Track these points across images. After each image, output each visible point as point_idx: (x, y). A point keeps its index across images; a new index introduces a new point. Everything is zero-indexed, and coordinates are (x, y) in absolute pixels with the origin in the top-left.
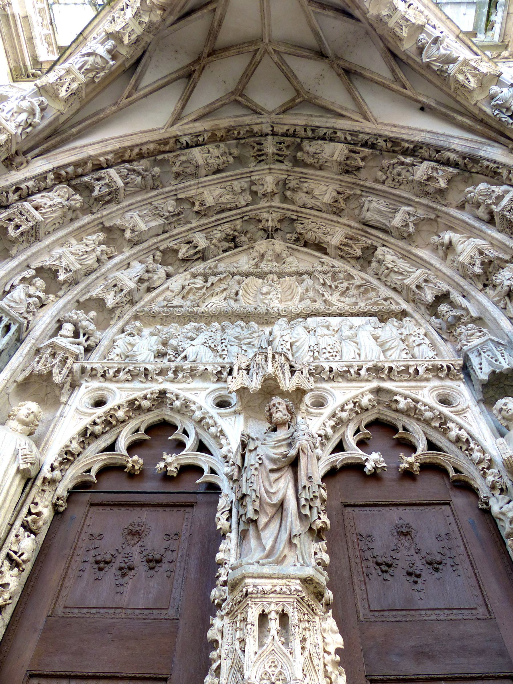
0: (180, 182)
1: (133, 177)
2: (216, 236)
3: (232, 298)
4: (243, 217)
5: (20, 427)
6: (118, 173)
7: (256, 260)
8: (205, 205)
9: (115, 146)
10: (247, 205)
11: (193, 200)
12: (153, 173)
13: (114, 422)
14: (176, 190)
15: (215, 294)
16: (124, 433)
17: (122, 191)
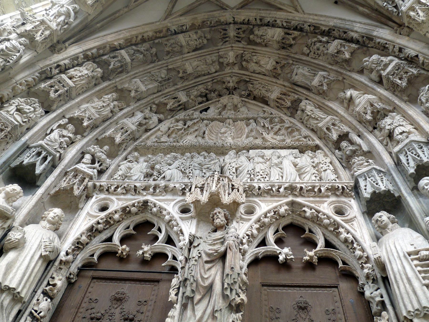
0: (170, 58)
1: (137, 55)
2: (193, 93)
3: (201, 136)
4: (213, 80)
5: (48, 226)
7: (219, 110)
8: (187, 73)
10: (216, 72)
11: (179, 69)
12: (151, 52)
13: (112, 222)
14: (167, 63)
15: (189, 133)
16: (118, 230)
17: (129, 65)
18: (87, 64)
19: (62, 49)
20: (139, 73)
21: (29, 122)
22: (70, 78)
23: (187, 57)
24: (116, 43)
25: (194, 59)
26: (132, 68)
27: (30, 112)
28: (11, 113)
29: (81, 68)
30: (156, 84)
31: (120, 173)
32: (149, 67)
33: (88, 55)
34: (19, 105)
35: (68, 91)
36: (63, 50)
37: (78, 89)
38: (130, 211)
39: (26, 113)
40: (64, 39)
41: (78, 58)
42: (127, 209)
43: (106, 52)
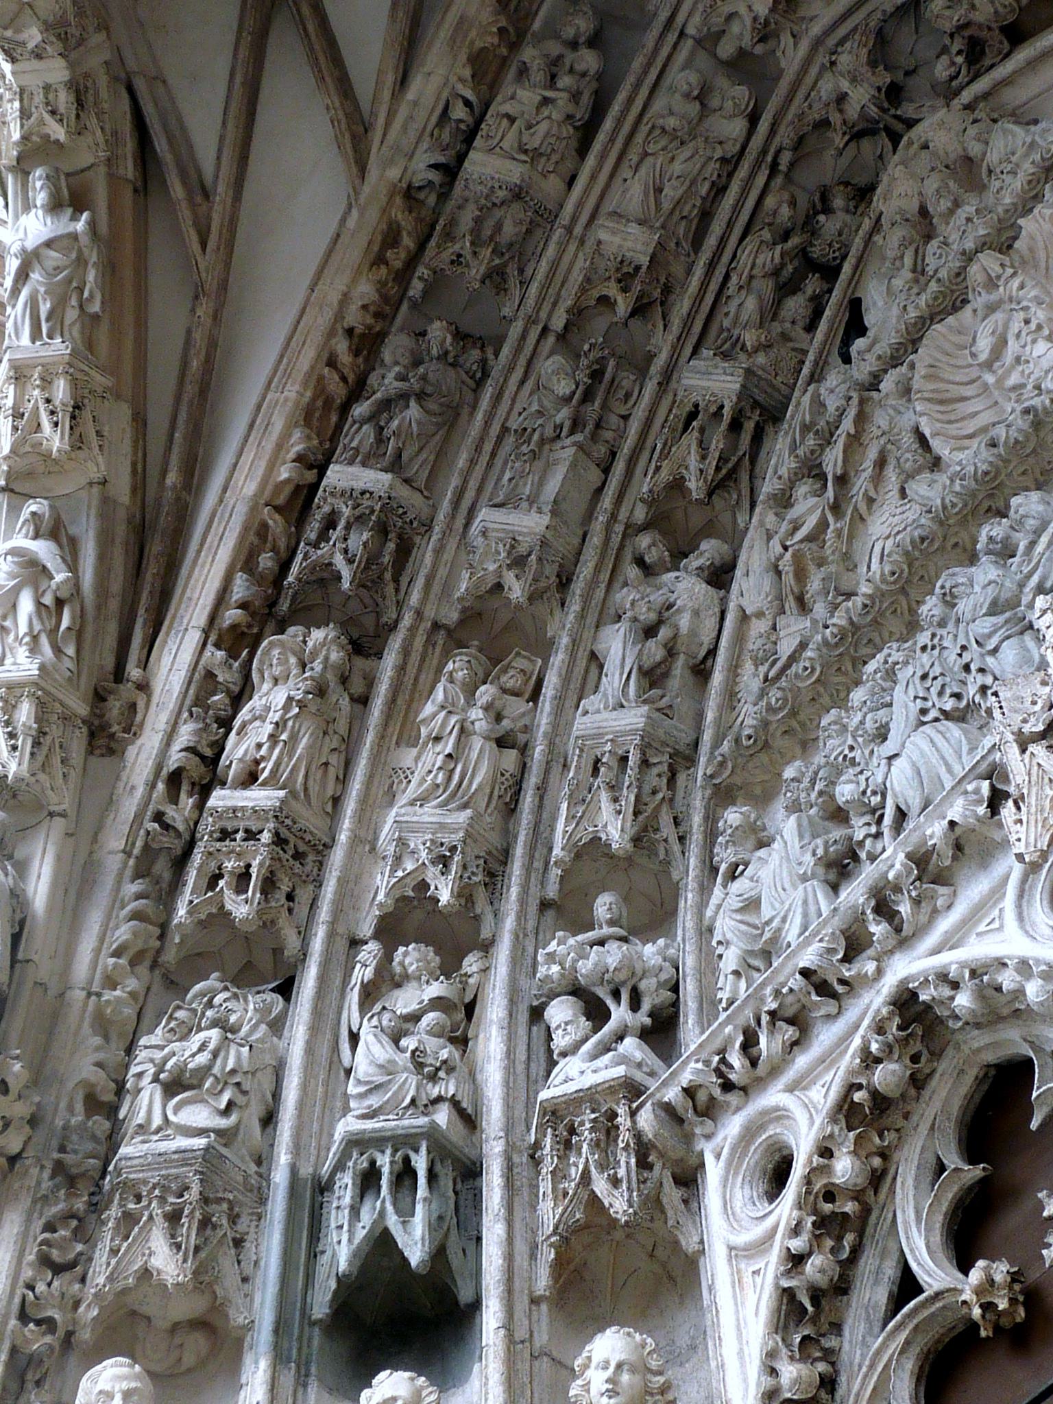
0: (525, 284)
1: (396, 423)
3: (919, 471)
4: (774, 167)
6: (351, 462)
7: (908, 260)
8: (638, 268)
9: (292, 394)
10: (753, 119)
11: (595, 294)
12: (434, 352)
14: (531, 321)
15: (862, 507)
17: (404, 492)
18: (261, 662)
19: (133, 707)
20: (465, 481)
21: (245, 1093)
22: (250, 778)
23: (580, 204)
24: (284, 473)
25: (618, 180)
26: (429, 489)
27: (215, 1054)
28: (157, 1121)
29: (256, 703)
30: (565, 453)
31: (730, 960)
32: (480, 416)
33: (234, 627)
34: (161, 1069)
35: (284, 833)
36: (141, 705)
37: (314, 788)
38: (875, 1094)
39: (206, 1070)
40: (109, 662)
41: (210, 675)
42: (858, 1096)
43: (282, 544)
